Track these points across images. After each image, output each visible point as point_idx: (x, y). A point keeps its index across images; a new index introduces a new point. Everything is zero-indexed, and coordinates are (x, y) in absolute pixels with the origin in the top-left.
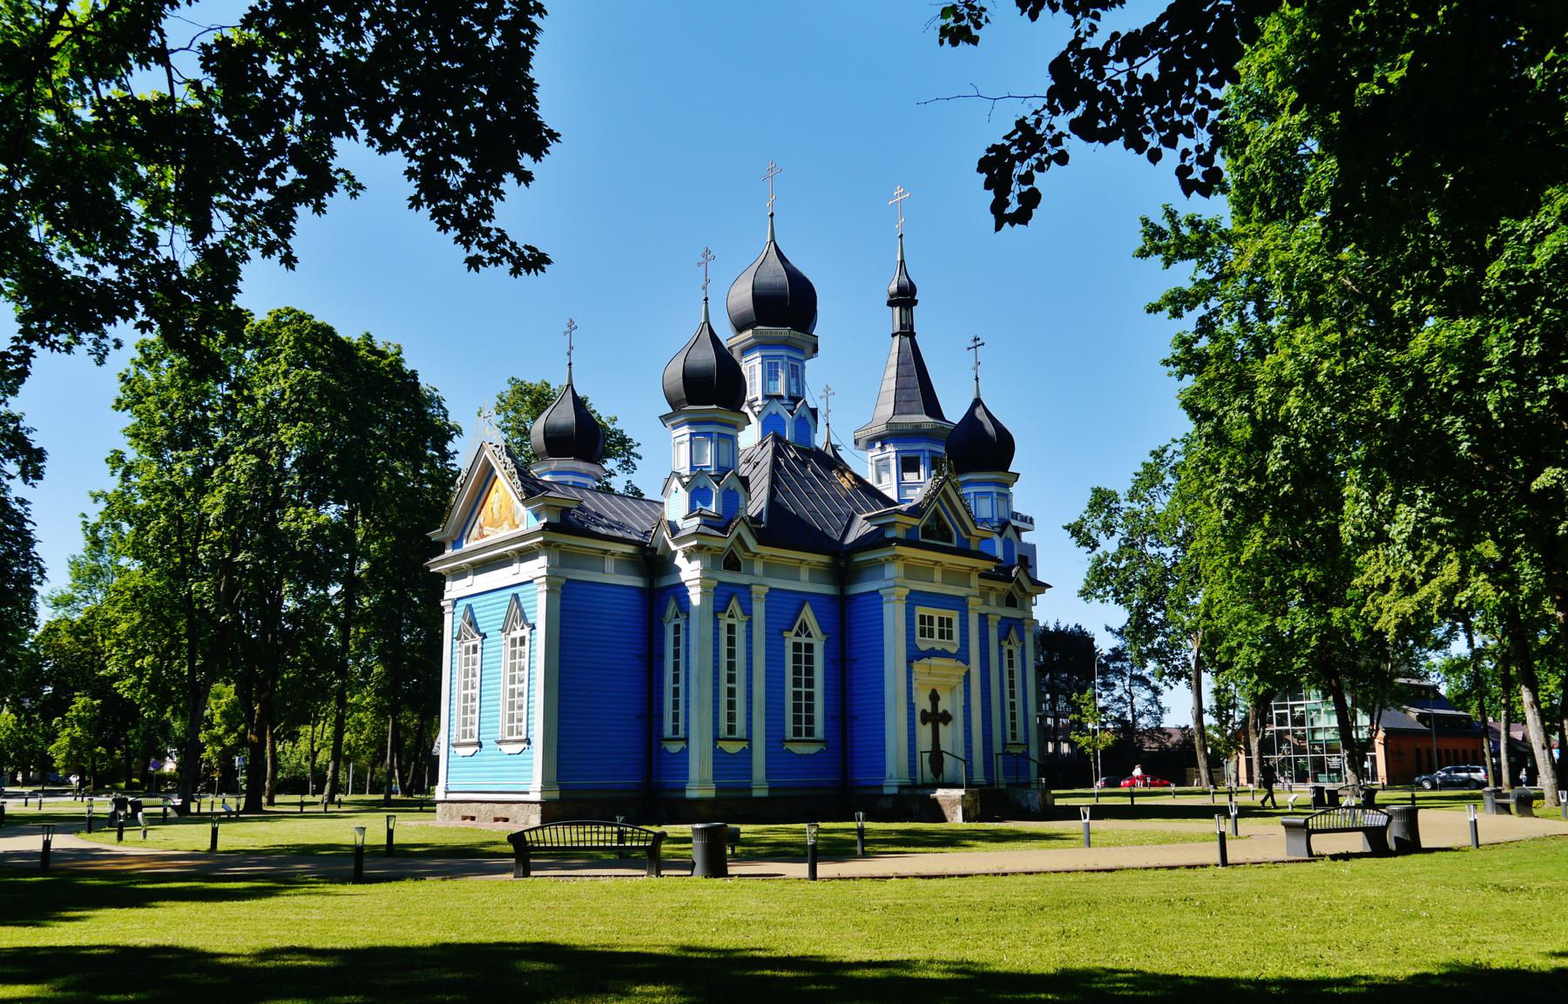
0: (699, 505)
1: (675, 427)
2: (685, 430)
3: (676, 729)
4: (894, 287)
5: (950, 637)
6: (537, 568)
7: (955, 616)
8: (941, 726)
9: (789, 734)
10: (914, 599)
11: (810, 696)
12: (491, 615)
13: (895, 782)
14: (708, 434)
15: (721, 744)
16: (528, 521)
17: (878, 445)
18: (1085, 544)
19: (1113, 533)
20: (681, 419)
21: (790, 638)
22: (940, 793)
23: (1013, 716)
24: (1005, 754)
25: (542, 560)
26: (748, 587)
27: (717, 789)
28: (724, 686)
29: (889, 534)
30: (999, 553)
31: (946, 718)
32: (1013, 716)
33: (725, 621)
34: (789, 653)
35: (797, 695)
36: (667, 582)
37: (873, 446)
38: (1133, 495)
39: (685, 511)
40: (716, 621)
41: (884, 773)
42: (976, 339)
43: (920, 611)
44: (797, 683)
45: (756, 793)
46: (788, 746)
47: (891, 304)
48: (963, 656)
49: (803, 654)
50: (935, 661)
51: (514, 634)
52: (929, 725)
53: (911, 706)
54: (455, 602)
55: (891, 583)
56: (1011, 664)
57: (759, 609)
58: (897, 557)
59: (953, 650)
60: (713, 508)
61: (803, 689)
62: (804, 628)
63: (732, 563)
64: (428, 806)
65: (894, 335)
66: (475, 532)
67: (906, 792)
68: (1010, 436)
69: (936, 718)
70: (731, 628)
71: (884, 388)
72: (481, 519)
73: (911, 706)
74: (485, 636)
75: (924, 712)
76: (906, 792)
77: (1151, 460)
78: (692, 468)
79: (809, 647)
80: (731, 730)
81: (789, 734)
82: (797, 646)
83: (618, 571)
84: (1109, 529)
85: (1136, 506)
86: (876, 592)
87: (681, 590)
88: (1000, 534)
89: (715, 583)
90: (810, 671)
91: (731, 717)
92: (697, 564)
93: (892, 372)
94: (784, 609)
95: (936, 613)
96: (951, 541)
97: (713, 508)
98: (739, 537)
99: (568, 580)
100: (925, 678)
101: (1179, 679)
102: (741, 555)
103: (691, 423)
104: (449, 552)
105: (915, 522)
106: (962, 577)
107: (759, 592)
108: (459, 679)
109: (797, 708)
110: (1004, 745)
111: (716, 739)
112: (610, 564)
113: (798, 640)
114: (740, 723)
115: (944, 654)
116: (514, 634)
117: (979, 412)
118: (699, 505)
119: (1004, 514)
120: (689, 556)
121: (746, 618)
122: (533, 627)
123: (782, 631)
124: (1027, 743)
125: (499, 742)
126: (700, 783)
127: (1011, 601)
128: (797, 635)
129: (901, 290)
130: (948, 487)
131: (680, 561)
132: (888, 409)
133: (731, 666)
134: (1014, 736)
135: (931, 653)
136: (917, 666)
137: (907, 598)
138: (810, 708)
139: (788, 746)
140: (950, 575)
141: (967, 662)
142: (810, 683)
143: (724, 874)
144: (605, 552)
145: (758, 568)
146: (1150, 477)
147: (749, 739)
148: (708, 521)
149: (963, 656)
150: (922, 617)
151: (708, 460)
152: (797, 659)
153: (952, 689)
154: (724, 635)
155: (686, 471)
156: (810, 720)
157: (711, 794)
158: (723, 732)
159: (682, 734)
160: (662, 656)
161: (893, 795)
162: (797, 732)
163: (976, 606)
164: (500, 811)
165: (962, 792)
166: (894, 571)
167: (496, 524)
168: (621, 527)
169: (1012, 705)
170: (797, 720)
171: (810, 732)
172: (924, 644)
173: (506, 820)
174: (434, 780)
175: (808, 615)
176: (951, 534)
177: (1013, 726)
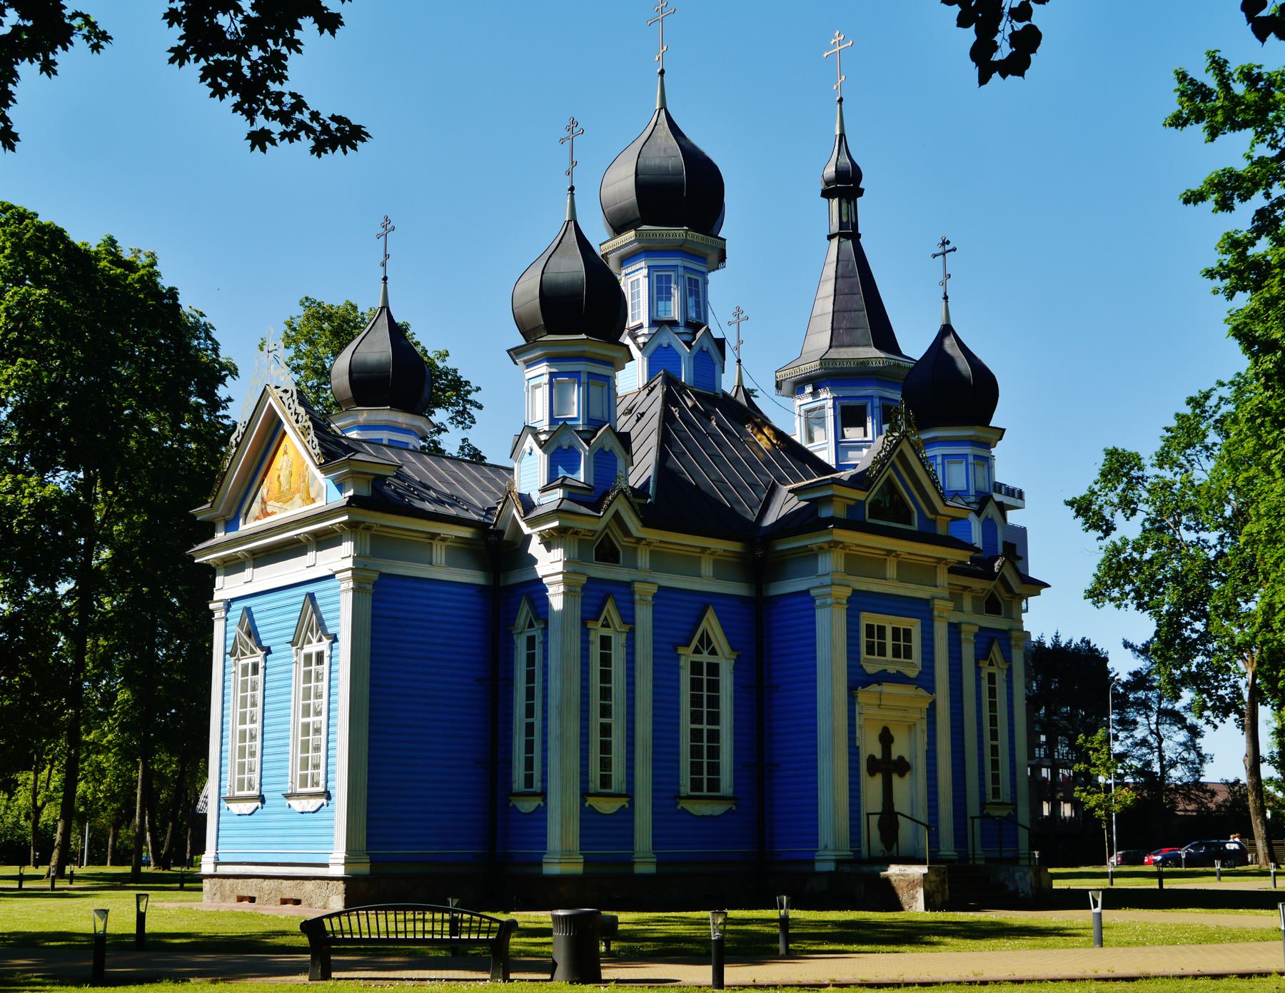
0: (562, 472)
1: (529, 364)
2: (543, 368)
3: (529, 780)
4: (830, 171)
5: (908, 654)
6: (340, 557)
7: (915, 626)
8: (896, 779)
9: (685, 788)
10: (859, 602)
11: (714, 736)
12: (277, 622)
13: (830, 855)
14: (574, 375)
15: (591, 801)
16: (327, 494)
17: (809, 389)
18: (1096, 527)
19: (1134, 512)
20: (538, 353)
21: (687, 656)
22: (894, 870)
23: (995, 764)
24: (984, 817)
25: (347, 548)
26: (628, 585)
27: (586, 863)
28: (596, 720)
29: (825, 513)
30: (977, 538)
31: (902, 767)
32: (995, 764)
33: (597, 632)
34: (685, 677)
35: (696, 735)
36: (517, 577)
37: (802, 391)
38: (1163, 459)
39: (542, 480)
40: (585, 632)
41: (816, 842)
42: (946, 243)
43: (867, 618)
44: (696, 718)
45: (639, 869)
46: (683, 804)
47: (826, 194)
48: (925, 681)
49: (706, 677)
50: (888, 688)
51: (308, 649)
52: (878, 778)
53: (854, 751)
54: (228, 604)
55: (827, 580)
56: (992, 692)
57: (644, 615)
58: (835, 544)
59: (913, 673)
60: (581, 476)
61: (705, 727)
62: (706, 642)
63: (607, 552)
64: (192, 882)
65: (830, 237)
66: (256, 508)
67: (847, 869)
68: (993, 377)
69: (889, 767)
70: (606, 642)
71: (817, 311)
72: (264, 490)
73: (854, 751)
74: (268, 651)
75: (871, 759)
76: (847, 869)
77: (1188, 410)
78: (553, 421)
79: (713, 669)
80: (605, 781)
81: (685, 788)
82: (696, 667)
83: (450, 563)
84: (1128, 506)
85: (1167, 474)
86: (807, 592)
87: (537, 588)
88: (978, 513)
89: (583, 580)
90: (714, 702)
91: (606, 764)
92: (558, 553)
93: (828, 288)
94: (678, 615)
95: (889, 622)
96: (910, 523)
97: (581, 476)
98: (617, 517)
99: (382, 575)
100: (872, 712)
101: (1226, 715)
102: (620, 541)
103: (551, 359)
104: (220, 536)
105: (860, 495)
106: (924, 572)
107: (644, 592)
108: (233, 710)
109: (696, 752)
110: (983, 804)
111: (585, 793)
112: (439, 553)
113: (697, 658)
114: (618, 773)
115: (900, 679)
116: (308, 649)
117: (949, 343)
118: (562, 472)
119: (983, 485)
120: (548, 542)
121: (626, 628)
122: (335, 639)
123: (675, 646)
124: (1014, 803)
125: (287, 796)
126: (562, 855)
127: (992, 606)
128: (697, 651)
129: (841, 174)
130: (905, 447)
131: (536, 548)
132: (822, 340)
133: (606, 694)
134: (996, 792)
135: (882, 677)
136: (863, 696)
137: (849, 600)
138: (714, 752)
139: (683, 804)
140: (908, 570)
141: (931, 689)
142: (714, 718)
143: (595, 978)
144: (433, 536)
145: (643, 559)
146: (1186, 433)
147: (630, 794)
148: (573, 493)
149: (925, 681)
150: (870, 628)
151: (574, 410)
152: (696, 685)
153: (911, 728)
154: (595, 651)
155: (544, 425)
156: (714, 769)
157: (578, 869)
158: (595, 785)
159: (537, 786)
160: (510, 680)
161: (828, 874)
162: (696, 785)
163: (943, 610)
164: (289, 889)
165: (924, 869)
166: (829, 563)
167: (284, 497)
168: (455, 501)
169: (994, 750)
170: (696, 768)
171: (714, 785)
172: (872, 665)
173: (297, 902)
174: (200, 848)
175: (711, 624)
176: (910, 513)
177: (996, 779)
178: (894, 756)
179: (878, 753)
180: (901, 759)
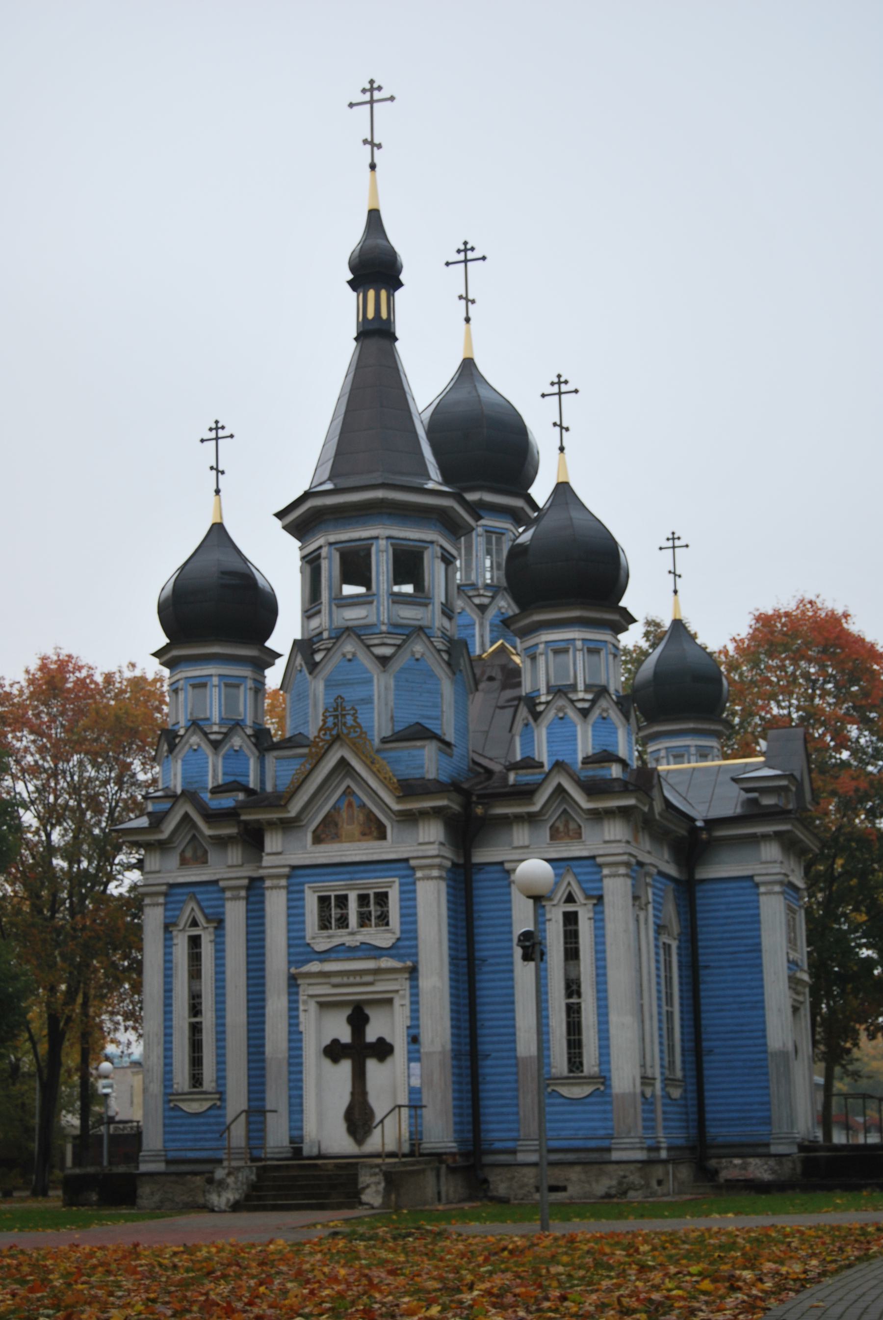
5: (383, 919)
8: (372, 1065)
31: (383, 1050)
52: (346, 1067)
75: (335, 1042)
179: (345, 1035)
180: (381, 1040)
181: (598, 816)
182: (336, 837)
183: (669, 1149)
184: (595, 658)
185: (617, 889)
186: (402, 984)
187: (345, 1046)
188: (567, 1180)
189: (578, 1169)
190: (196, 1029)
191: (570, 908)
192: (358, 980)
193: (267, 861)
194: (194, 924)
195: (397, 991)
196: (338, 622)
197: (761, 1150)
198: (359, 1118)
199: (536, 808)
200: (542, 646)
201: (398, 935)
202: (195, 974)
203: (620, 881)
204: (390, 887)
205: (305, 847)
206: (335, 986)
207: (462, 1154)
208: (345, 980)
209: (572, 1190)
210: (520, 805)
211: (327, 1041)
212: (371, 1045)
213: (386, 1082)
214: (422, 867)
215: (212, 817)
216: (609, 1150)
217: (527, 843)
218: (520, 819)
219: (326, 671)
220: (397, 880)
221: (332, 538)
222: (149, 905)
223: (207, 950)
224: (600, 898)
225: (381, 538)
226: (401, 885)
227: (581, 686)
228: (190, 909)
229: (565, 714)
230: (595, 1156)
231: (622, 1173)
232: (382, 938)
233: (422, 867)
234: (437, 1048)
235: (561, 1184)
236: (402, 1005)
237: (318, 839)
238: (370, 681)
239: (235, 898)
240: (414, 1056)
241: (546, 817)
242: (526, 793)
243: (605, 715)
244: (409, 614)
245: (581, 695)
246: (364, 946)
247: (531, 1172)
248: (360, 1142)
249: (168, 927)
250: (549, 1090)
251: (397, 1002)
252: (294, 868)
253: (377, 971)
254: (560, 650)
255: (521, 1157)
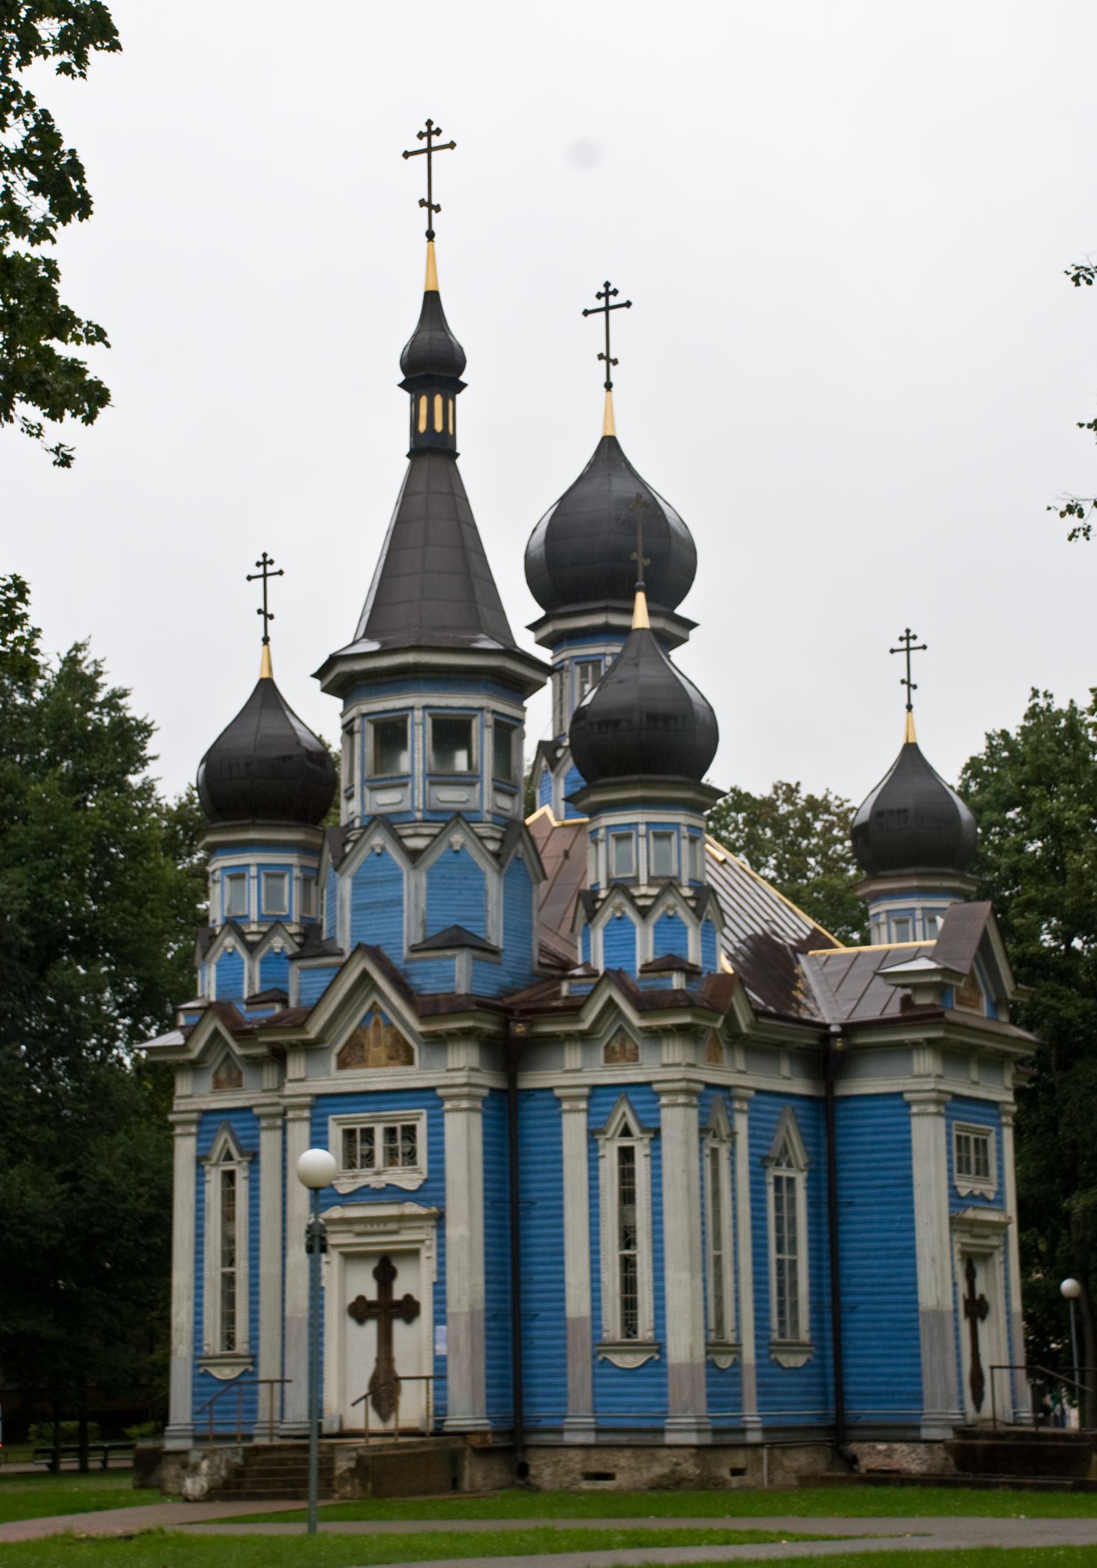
5: (411, 1156)
31: (409, 1309)
52: (371, 1328)
75: (361, 1299)
178: (398, 1295)
179: (371, 1292)
180: (408, 1298)
181: (656, 1035)
182: (363, 1062)
183: (765, 1430)
184: (664, 844)
185: (678, 1123)
186: (426, 1234)
187: (371, 1305)
188: (615, 1466)
189: (628, 1453)
190: (229, 1280)
191: (626, 1143)
192: (382, 1228)
193: (290, 1088)
194: (229, 1157)
195: (422, 1241)
196: (371, 809)
197: (911, 1434)
198: (384, 1390)
199: (585, 1026)
200: (602, 832)
201: (425, 1176)
202: (228, 1217)
203: (679, 1112)
204: (417, 1119)
205: (328, 1073)
206: (359, 1234)
207: (494, 1433)
208: (369, 1228)
209: (622, 1480)
210: (568, 1022)
211: (351, 1299)
212: (398, 1304)
213: (413, 1344)
214: (451, 1098)
215: (243, 1034)
216: (662, 1431)
217: (579, 1066)
218: (570, 1037)
219: (354, 866)
220: (424, 1111)
221: (365, 708)
222: (181, 1135)
223: (241, 1187)
224: (657, 1132)
225: (418, 705)
226: (429, 1117)
227: (643, 879)
228: (223, 1140)
229: (623, 913)
230: (647, 1439)
231: (674, 1460)
232: (408, 1179)
233: (451, 1098)
234: (464, 1308)
235: (609, 1471)
236: (429, 1258)
237: (343, 1064)
238: (398, 879)
239: (270, 1128)
240: (440, 1318)
241: (600, 1036)
242: (574, 1009)
243: (671, 913)
244: (450, 796)
245: (644, 890)
246: (390, 1188)
247: (577, 1455)
248: (384, 1417)
249: (200, 1161)
250: (600, 1358)
251: (424, 1254)
252: (319, 1096)
253: (401, 1218)
254: (623, 836)
255: (568, 1438)
